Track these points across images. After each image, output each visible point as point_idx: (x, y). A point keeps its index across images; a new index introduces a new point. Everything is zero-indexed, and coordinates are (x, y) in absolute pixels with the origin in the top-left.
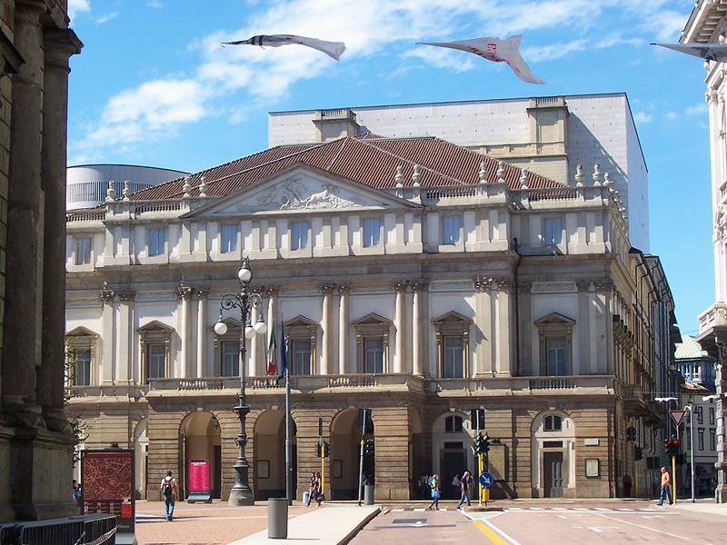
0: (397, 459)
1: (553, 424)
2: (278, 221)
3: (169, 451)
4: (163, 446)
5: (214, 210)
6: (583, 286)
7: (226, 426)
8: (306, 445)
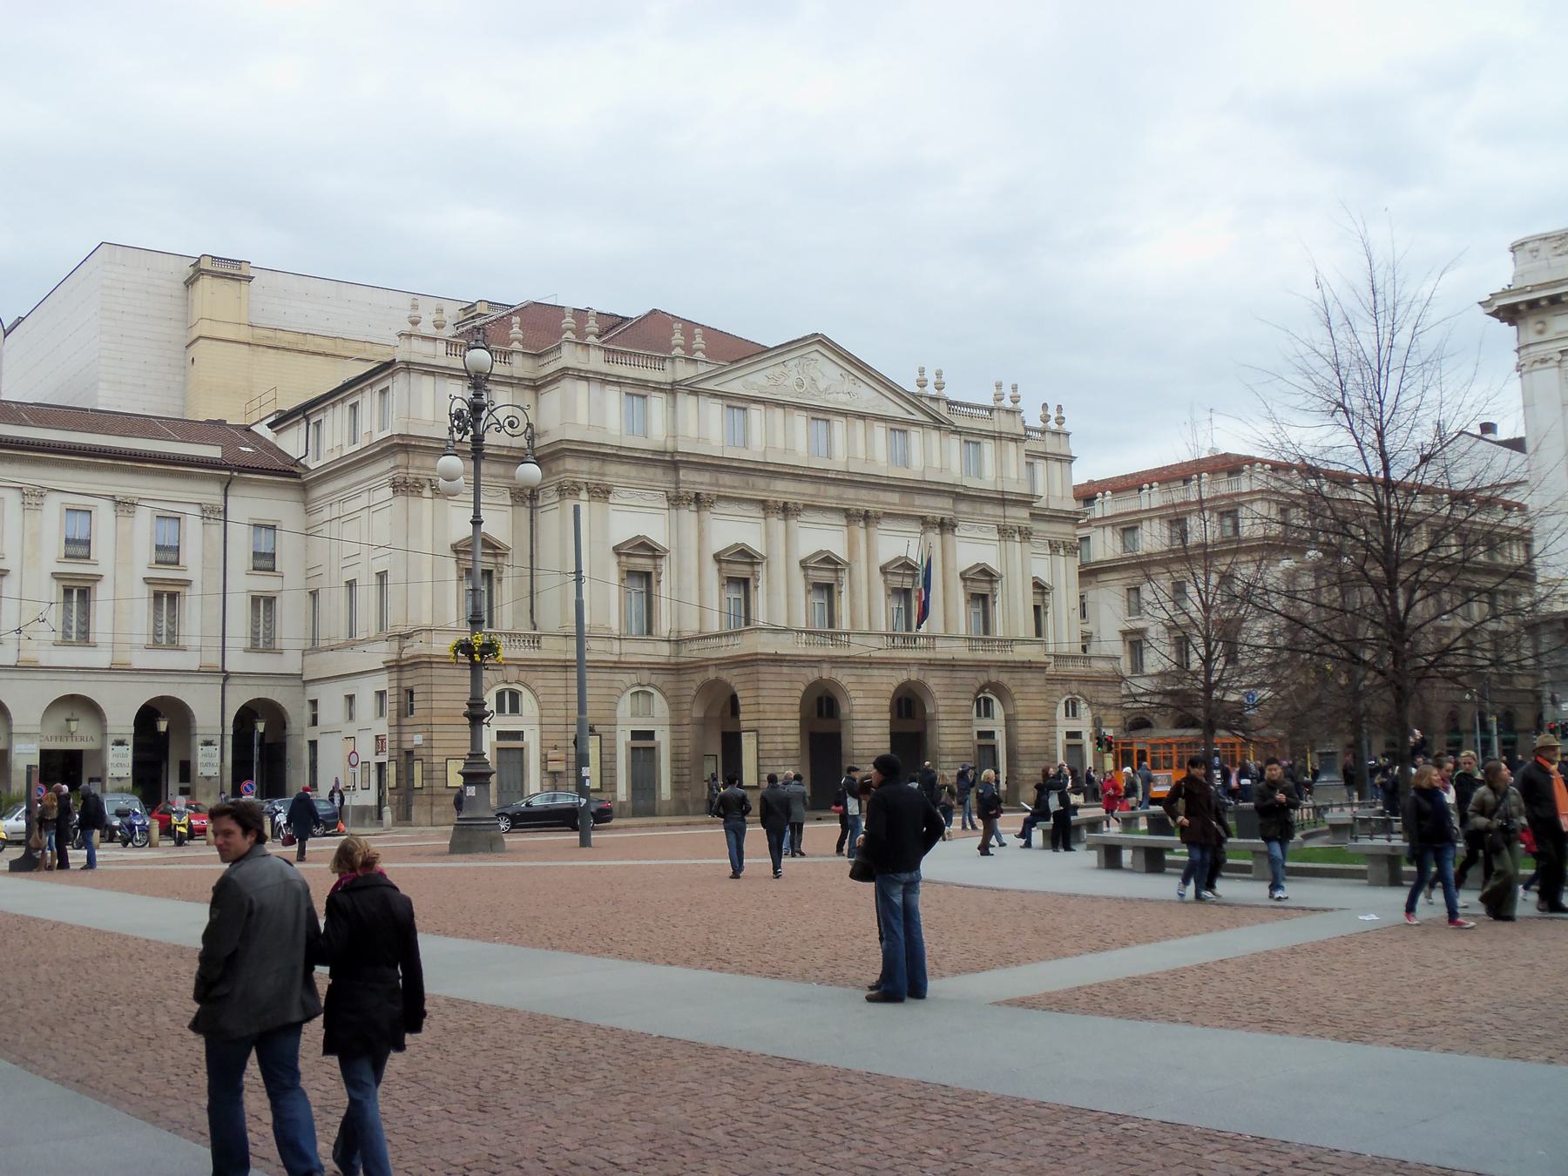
1: (1072, 710)
2: (797, 412)
4: (779, 731)
5: (717, 381)
6: (1054, 547)
7: (857, 701)
8: (947, 731)
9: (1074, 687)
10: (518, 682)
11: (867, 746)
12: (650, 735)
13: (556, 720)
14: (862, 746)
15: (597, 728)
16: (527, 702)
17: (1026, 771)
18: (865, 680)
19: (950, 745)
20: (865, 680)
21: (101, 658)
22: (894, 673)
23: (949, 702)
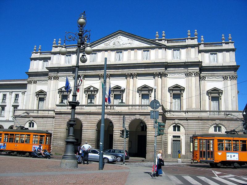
11: (87, 137)
14: (85, 137)
23: (118, 125)
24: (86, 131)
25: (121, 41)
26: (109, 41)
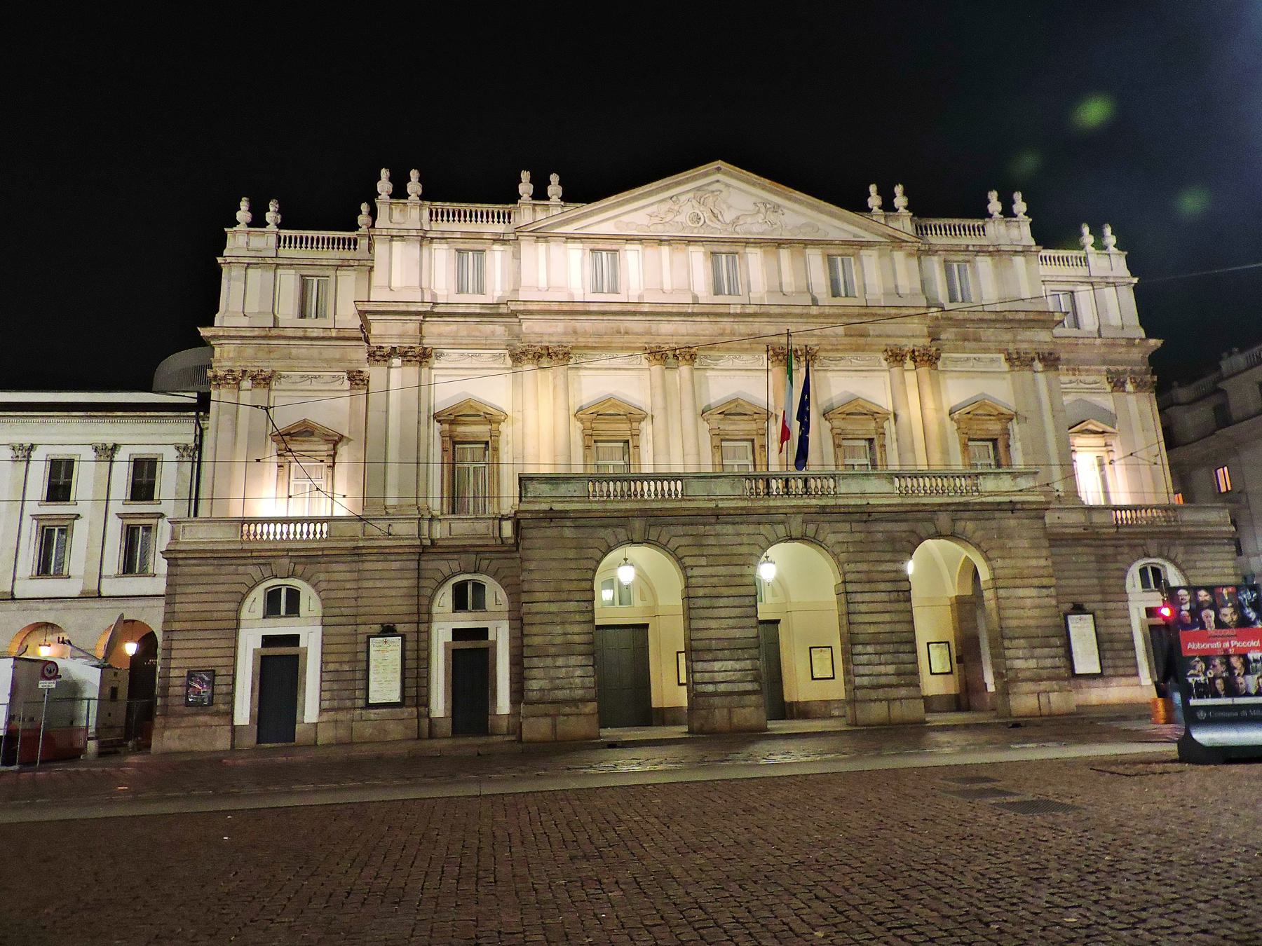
0: (1039, 632)
3: (569, 628)
7: (696, 572)
8: (863, 608)
9: (1152, 546)
10: (292, 575)
12: (482, 633)
13: (344, 620)
15: (400, 628)
16: (310, 602)
17: (1019, 664)
18: (712, 541)
19: (872, 629)
20: (712, 541)
21: (71, 588)
22: (762, 529)
24: (705, 602)
25: (724, 206)
26: (669, 204)
